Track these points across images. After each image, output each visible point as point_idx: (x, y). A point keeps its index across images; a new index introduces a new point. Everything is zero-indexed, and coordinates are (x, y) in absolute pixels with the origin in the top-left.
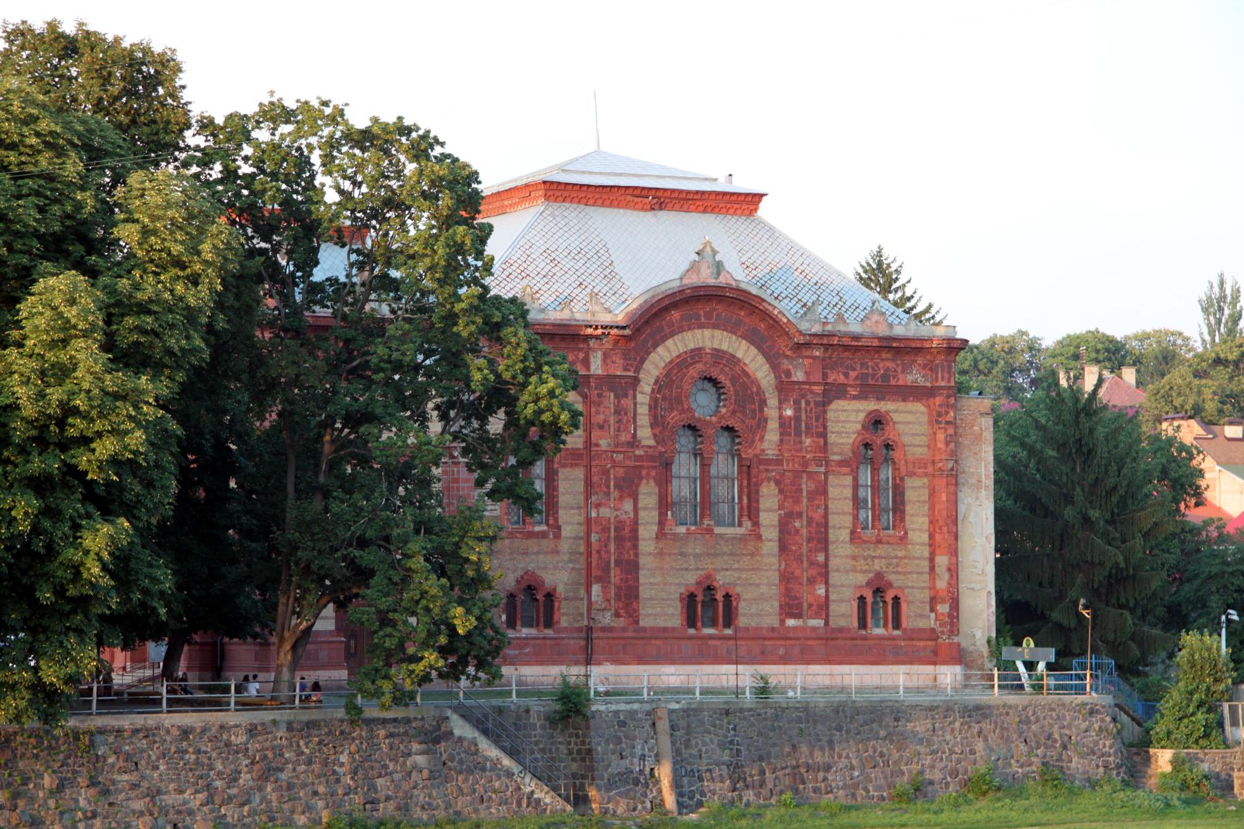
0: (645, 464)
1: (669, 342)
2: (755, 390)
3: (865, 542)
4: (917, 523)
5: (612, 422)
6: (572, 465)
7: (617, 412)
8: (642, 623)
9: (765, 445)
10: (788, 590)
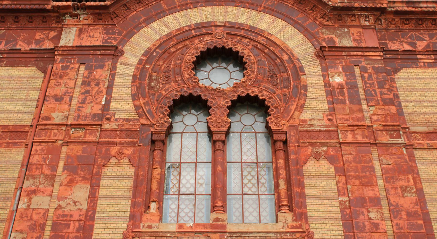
0: (118, 139)
1: (169, 19)
2: (285, 57)
6: (8, 145)
7: (86, 83)
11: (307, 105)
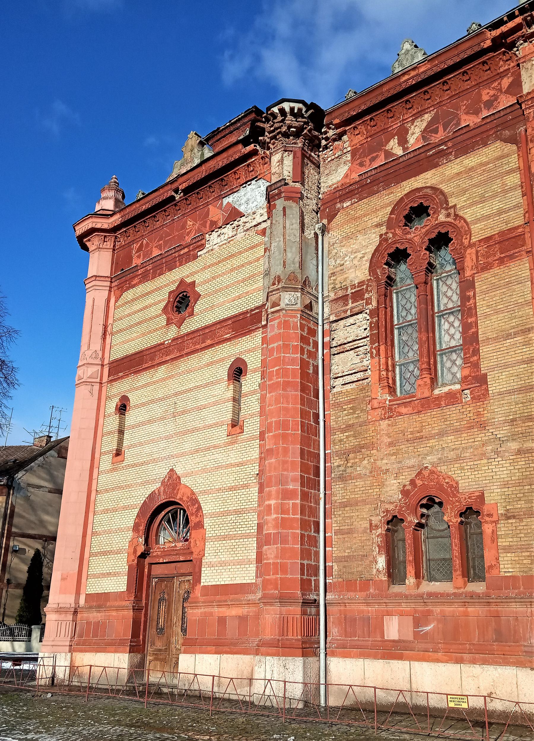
6: (502, 261)
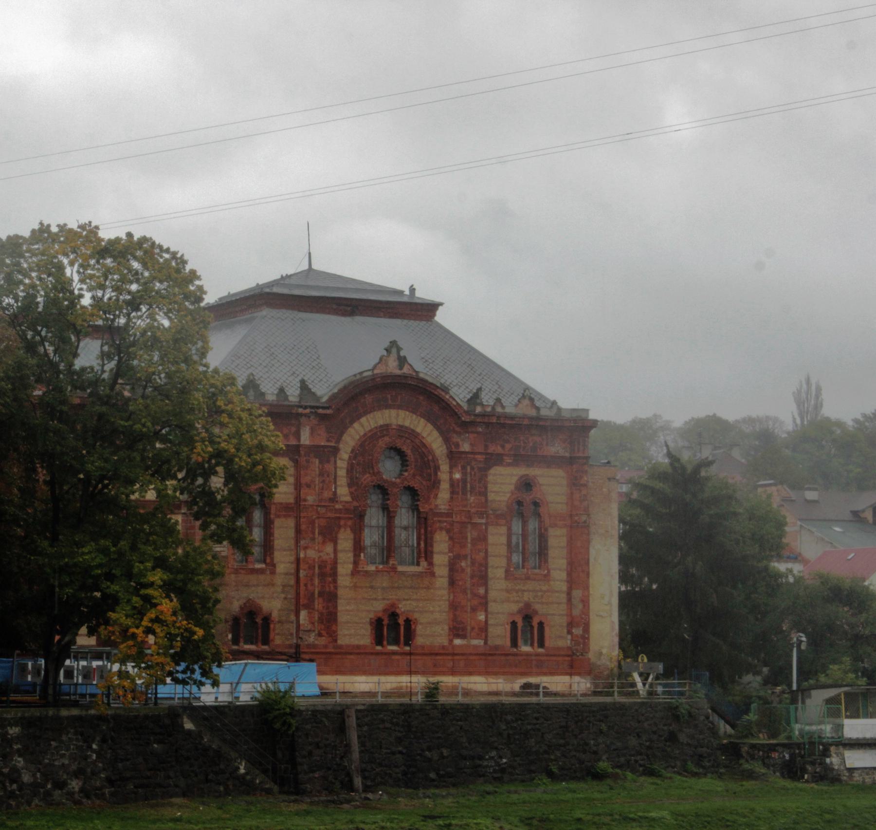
1: (363, 420)
2: (430, 458)
3: (516, 579)
4: (558, 560)
5: (317, 482)
6: (286, 516)
7: (321, 474)
8: (339, 642)
9: (439, 502)
10: (455, 619)
11: (440, 495)
